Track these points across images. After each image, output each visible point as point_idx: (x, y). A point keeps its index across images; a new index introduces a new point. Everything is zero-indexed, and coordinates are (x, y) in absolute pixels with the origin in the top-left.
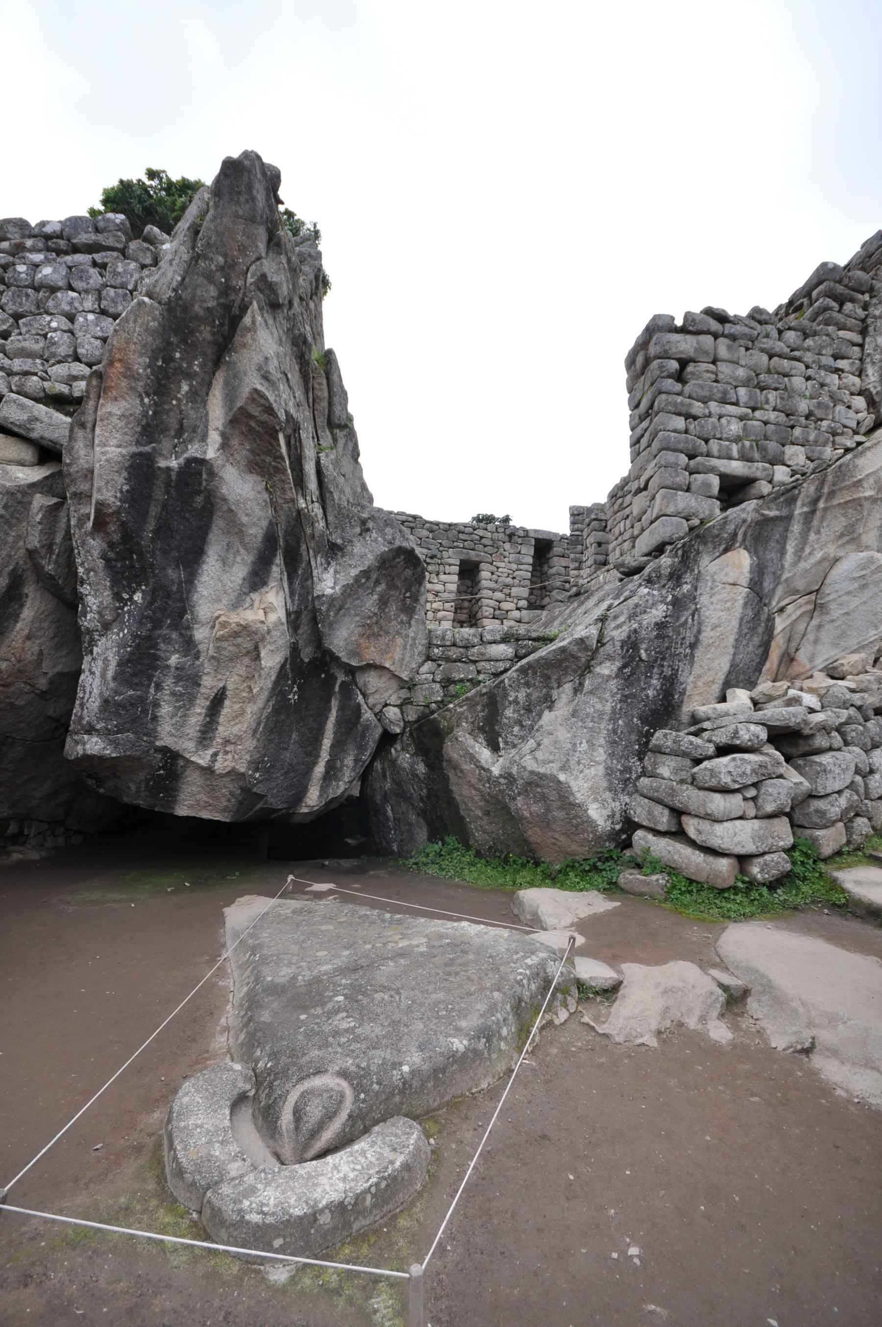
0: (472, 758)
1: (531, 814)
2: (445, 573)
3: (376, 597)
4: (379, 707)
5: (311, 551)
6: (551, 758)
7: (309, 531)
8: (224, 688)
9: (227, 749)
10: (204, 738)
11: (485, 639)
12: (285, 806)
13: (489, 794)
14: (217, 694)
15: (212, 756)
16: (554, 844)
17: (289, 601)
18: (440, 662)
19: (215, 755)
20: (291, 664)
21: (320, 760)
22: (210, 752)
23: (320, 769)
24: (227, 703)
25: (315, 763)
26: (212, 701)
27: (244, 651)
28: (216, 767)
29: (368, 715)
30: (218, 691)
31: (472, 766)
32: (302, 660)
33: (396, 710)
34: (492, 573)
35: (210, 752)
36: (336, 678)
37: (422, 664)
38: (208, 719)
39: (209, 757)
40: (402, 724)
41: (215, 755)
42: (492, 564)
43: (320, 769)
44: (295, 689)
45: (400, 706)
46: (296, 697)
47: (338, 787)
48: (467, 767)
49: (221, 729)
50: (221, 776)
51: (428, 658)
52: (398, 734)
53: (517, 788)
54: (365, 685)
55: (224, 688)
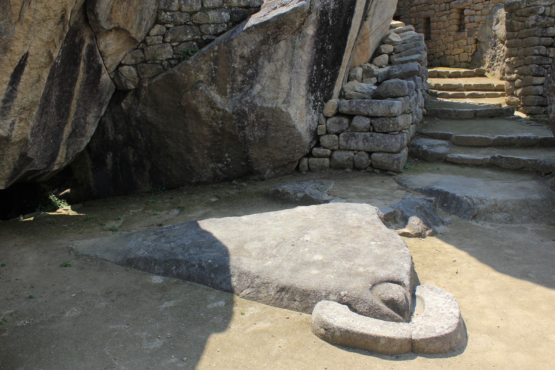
0: (212, 104)
1: (255, 138)
4: (114, 67)
6: (275, 95)
9: (23, 116)
10: (5, 108)
11: (205, 6)
12: (45, 166)
13: (220, 129)
14: (20, 61)
15: (11, 125)
16: (268, 156)
18: (169, 26)
19: (13, 123)
23: (67, 130)
24: (26, 69)
26: (16, 69)
28: (13, 136)
29: (105, 77)
30: (23, 57)
31: (208, 108)
33: (132, 69)
37: (153, 27)
38: (10, 88)
40: (137, 80)
41: (13, 123)
43: (67, 130)
45: (135, 66)
47: (82, 142)
48: (203, 110)
49: (19, 96)
50: (13, 144)
51: (157, 22)
52: (130, 90)
53: (247, 120)
54: (106, 46)
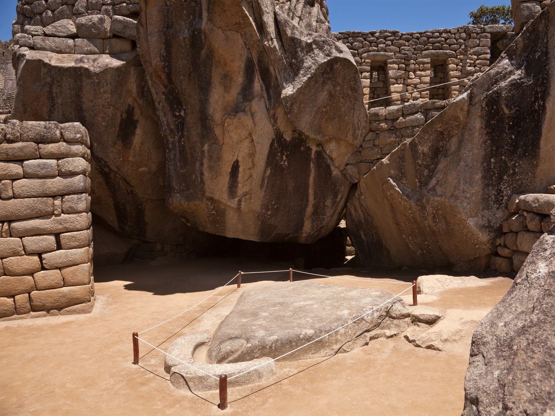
2: (420, 70)
3: (325, 93)
5: (276, 70)
7: (272, 57)
8: (237, 162)
17: (267, 102)
19: (240, 201)
20: (277, 143)
21: (309, 203)
22: (237, 199)
24: (241, 169)
25: (306, 205)
27: (243, 137)
32: (285, 140)
34: (457, 65)
35: (237, 199)
36: (311, 149)
37: (367, 135)
39: (236, 202)
41: (240, 201)
42: (456, 58)
43: (310, 209)
44: (285, 158)
46: (286, 163)
55: (237, 162)
